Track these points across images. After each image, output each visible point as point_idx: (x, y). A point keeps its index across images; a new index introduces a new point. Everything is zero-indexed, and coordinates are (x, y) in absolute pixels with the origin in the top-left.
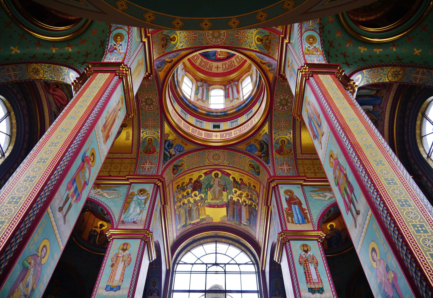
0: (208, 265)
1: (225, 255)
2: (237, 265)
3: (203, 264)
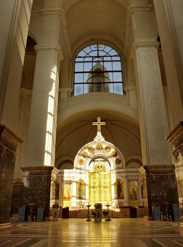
1: (103, 51)
3: (90, 57)
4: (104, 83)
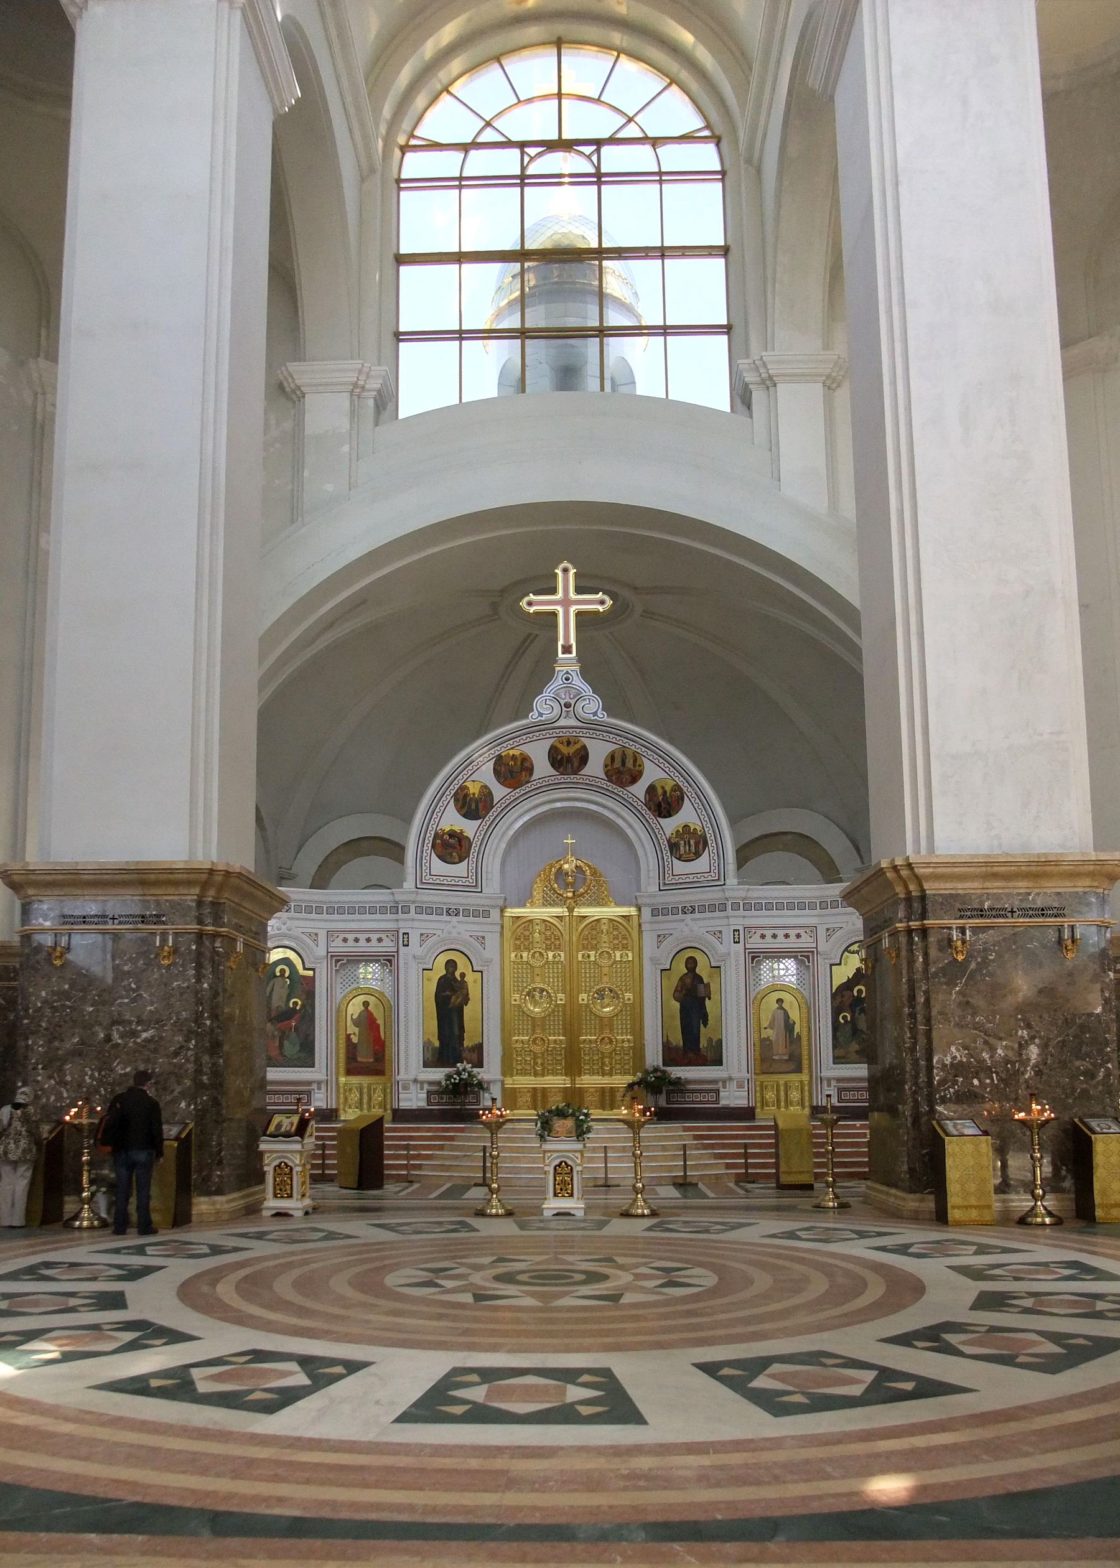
0: (526, 150)
1: (598, 101)
2: (647, 149)
3: (508, 144)
4: (602, 332)
